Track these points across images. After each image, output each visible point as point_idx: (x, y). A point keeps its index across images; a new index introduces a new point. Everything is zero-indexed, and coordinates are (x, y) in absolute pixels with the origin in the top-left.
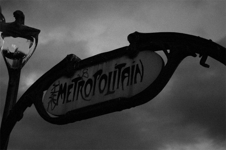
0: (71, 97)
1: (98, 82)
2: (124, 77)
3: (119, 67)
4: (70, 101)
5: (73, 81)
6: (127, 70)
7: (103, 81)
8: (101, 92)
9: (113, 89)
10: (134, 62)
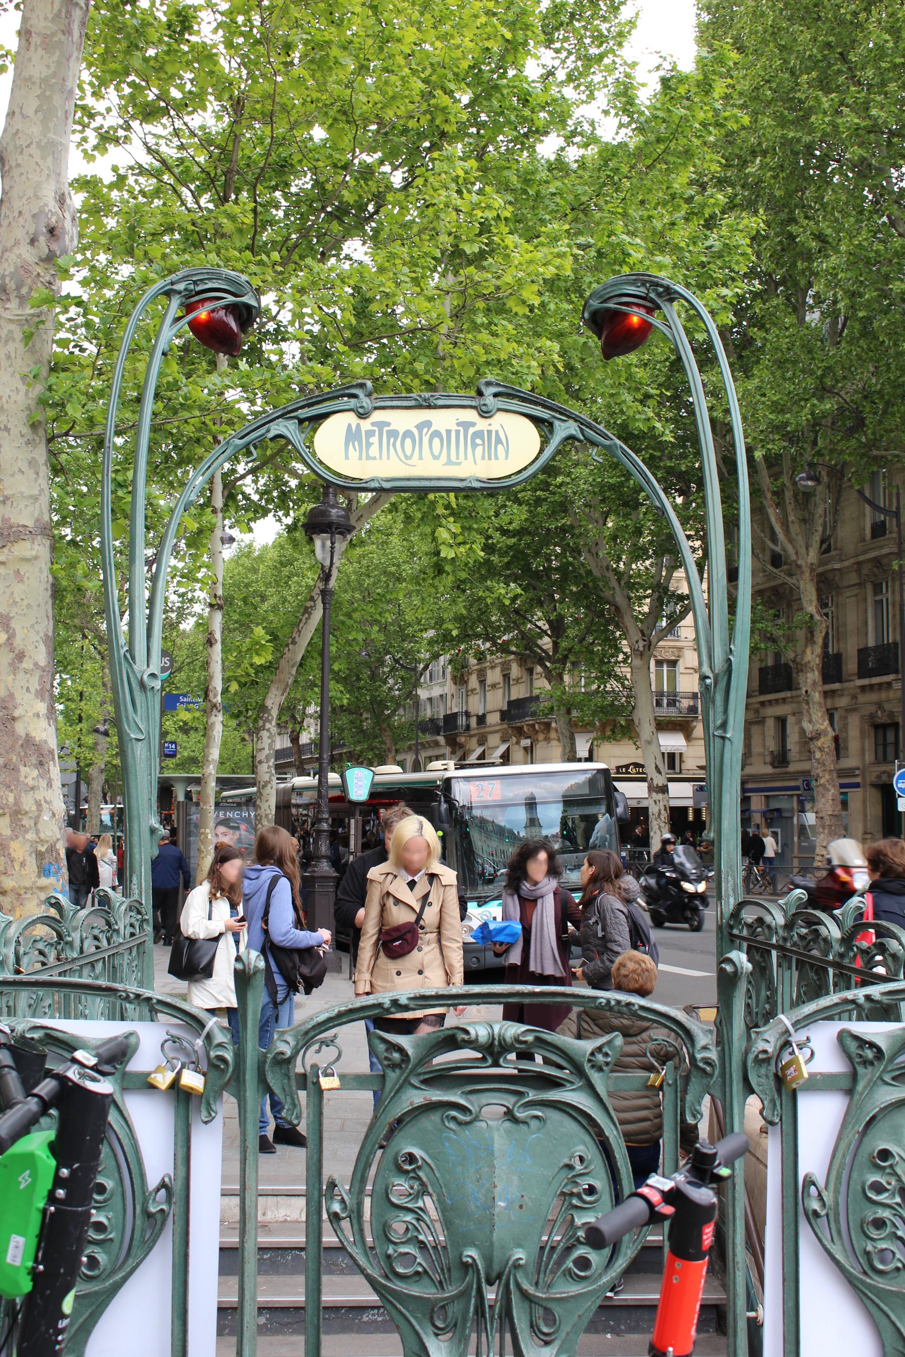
0: (374, 451)
1: (426, 439)
2: (474, 446)
3: (466, 425)
7: (436, 441)
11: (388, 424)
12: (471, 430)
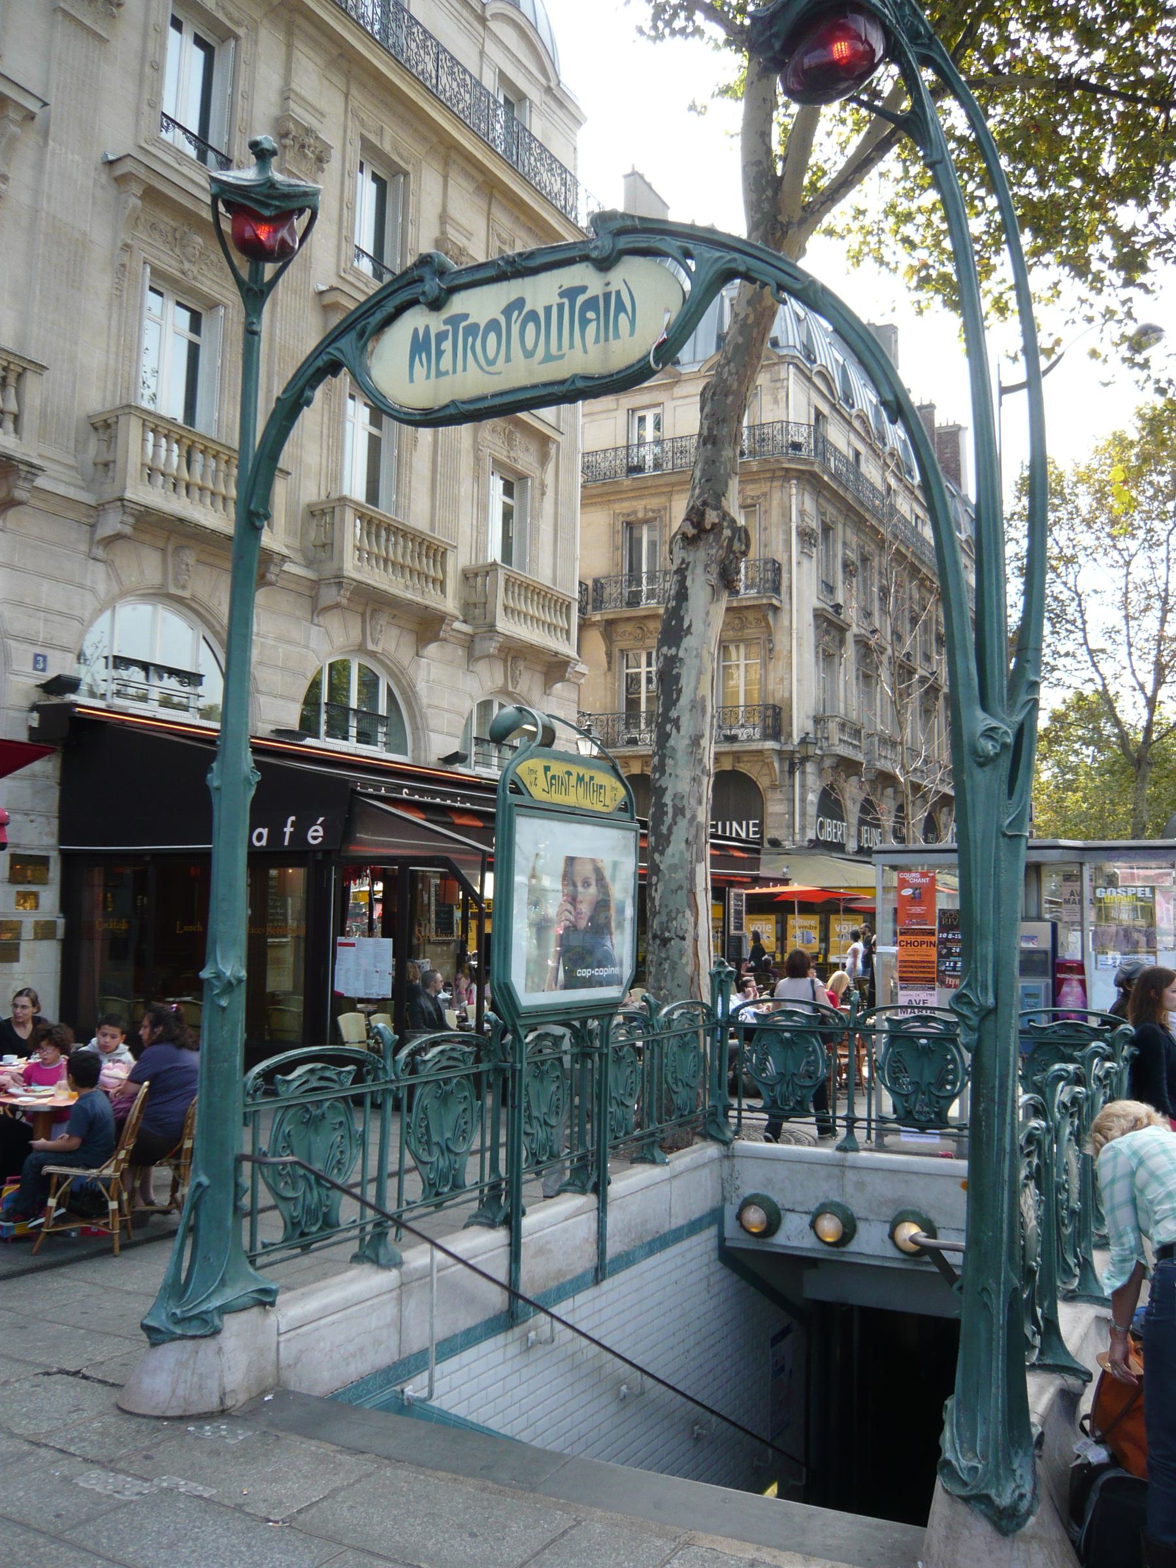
0: (446, 362)
1: (515, 329)
2: (584, 322)
3: (571, 293)
4: (447, 373)
5: (446, 322)
6: (592, 303)
7: (531, 327)
8: (529, 354)
9: (560, 347)
10: (608, 284)
11: (465, 316)
12: (581, 299)
